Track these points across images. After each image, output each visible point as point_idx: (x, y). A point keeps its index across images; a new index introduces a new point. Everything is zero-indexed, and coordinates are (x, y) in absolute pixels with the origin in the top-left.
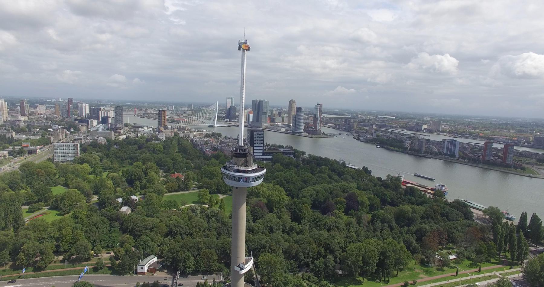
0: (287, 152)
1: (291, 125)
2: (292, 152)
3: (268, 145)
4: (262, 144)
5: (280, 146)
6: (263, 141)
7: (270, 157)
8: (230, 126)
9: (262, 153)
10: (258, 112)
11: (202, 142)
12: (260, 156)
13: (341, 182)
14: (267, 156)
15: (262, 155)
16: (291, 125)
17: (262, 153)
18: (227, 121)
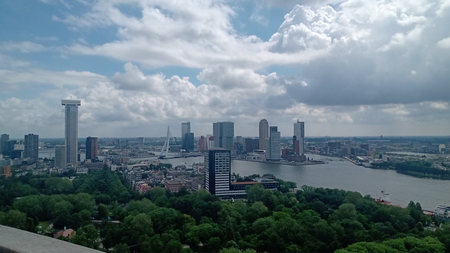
0: (267, 184)
1: (263, 151)
2: (275, 183)
3: (237, 176)
4: (227, 171)
5: (255, 176)
6: (229, 167)
7: (243, 192)
8: (186, 157)
9: (229, 186)
10: (221, 138)
11: (138, 175)
12: (226, 192)
13: (402, 237)
14: (237, 191)
15: (228, 189)
16: (265, 151)
17: (229, 186)
18: (183, 152)
